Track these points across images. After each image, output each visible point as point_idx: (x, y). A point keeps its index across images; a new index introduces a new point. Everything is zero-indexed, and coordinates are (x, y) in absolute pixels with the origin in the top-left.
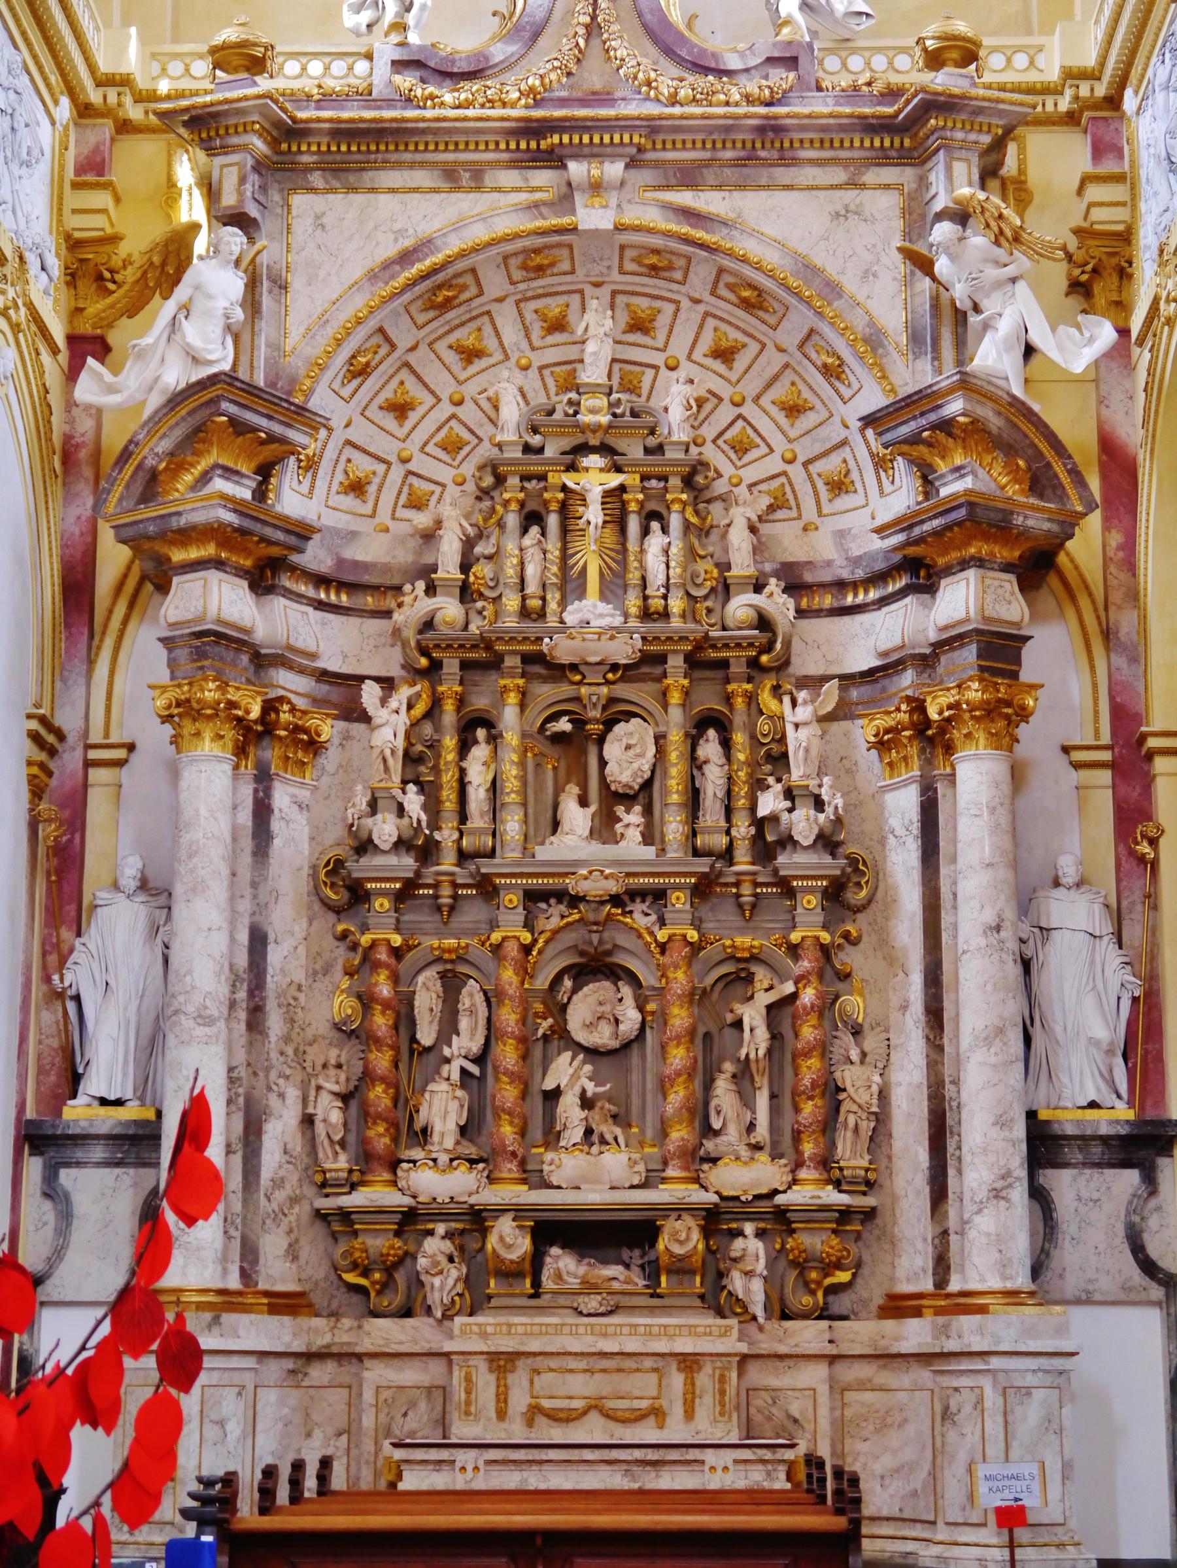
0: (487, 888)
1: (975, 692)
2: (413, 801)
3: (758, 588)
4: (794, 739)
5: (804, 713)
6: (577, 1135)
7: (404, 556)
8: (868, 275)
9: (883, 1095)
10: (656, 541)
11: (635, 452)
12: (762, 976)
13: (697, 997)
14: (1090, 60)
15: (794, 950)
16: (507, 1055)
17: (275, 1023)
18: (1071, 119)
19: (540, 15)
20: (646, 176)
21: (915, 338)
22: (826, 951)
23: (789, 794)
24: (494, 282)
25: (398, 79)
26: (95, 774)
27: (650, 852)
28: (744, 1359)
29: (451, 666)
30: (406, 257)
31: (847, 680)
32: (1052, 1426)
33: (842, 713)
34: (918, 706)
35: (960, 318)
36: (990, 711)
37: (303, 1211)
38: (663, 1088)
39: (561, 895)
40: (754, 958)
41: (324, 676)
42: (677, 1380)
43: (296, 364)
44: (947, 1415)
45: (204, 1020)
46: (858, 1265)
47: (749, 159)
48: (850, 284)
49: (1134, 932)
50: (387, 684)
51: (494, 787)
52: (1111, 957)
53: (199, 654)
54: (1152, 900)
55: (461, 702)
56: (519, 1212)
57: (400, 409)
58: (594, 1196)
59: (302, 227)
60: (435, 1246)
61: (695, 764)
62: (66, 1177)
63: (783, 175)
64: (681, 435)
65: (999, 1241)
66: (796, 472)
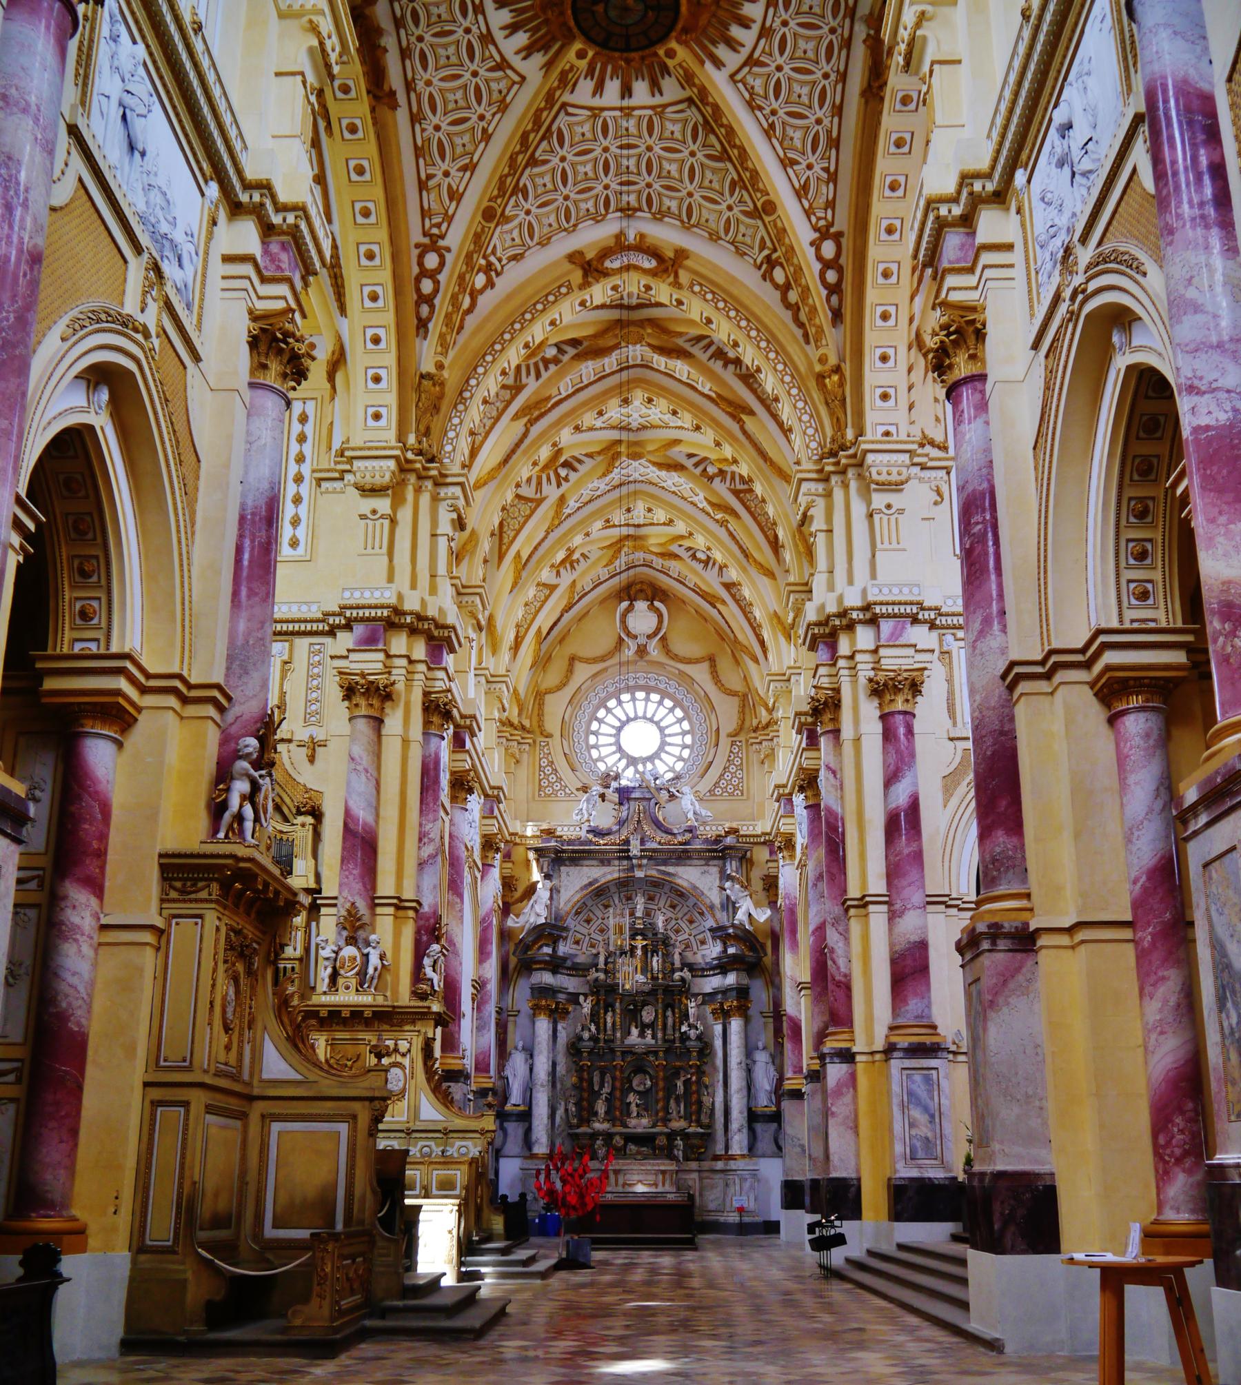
0: (612, 1051)
1: (735, 1003)
2: (593, 1028)
3: (681, 970)
4: (691, 1011)
5: (693, 1004)
6: (635, 1114)
7: (589, 960)
8: (710, 889)
9: (713, 1104)
10: (655, 959)
11: (650, 935)
12: (682, 1073)
13: (665, 1079)
14: (768, 830)
15: (691, 1067)
16: (618, 1094)
17: (559, 1086)
18: (764, 843)
20: (652, 862)
21: (722, 906)
22: (698, 1067)
23: (689, 1025)
24: (613, 889)
26: (511, 1018)
27: (653, 1042)
28: (677, 1172)
29: (602, 992)
30: (590, 884)
31: (705, 995)
32: (752, 1187)
33: (703, 1003)
34: (722, 1004)
35: (734, 903)
36: (739, 1008)
37: (565, 1134)
38: (657, 1101)
39: (631, 1052)
40: (681, 1068)
41: (569, 994)
42: (660, 1177)
43: (563, 913)
44: (727, 1185)
45: (542, 1086)
46: (706, 1148)
47: (679, 858)
48: (706, 892)
49: (777, 1061)
50: (586, 995)
51: (614, 1024)
52: (772, 1068)
53: (540, 993)
54: (782, 1053)
55: (605, 1000)
56: (621, 1134)
57: (588, 921)
58: (640, 1130)
59: (563, 875)
60: (599, 1142)
61: (665, 1017)
62: (506, 1124)
63: (688, 862)
64: (661, 931)
65: (740, 1142)
66: (692, 938)
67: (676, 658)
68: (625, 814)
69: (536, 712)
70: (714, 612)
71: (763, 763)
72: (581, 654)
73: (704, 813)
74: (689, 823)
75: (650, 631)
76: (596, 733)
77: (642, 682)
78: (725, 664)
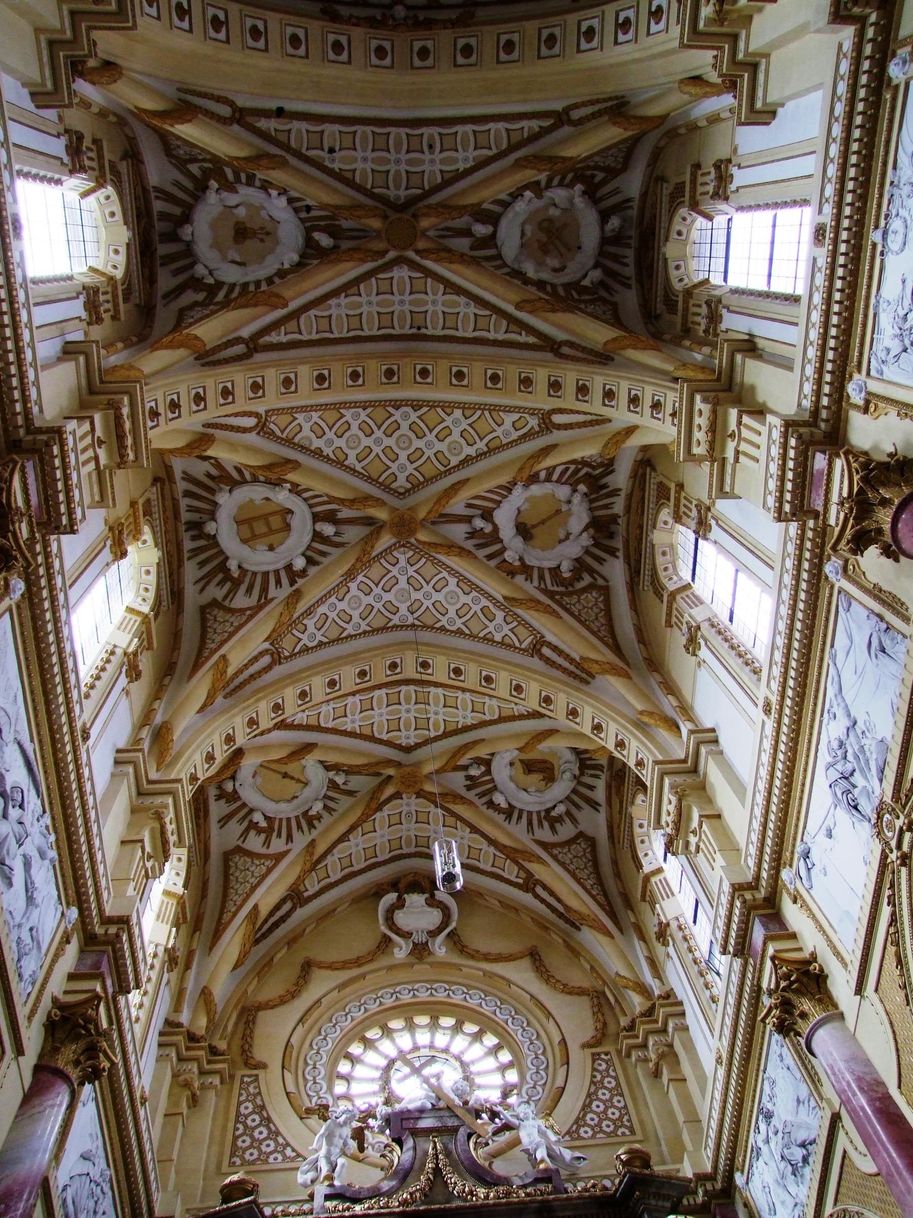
19: (407, 1165)
25: (328, 1204)
67: (475, 955)
68: (408, 1156)
69: (239, 1034)
70: (526, 898)
71: (657, 1074)
72: (320, 958)
73: (568, 1154)
74: (542, 1166)
75: (432, 928)
76: (347, 1078)
77: (423, 996)
78: (556, 961)
